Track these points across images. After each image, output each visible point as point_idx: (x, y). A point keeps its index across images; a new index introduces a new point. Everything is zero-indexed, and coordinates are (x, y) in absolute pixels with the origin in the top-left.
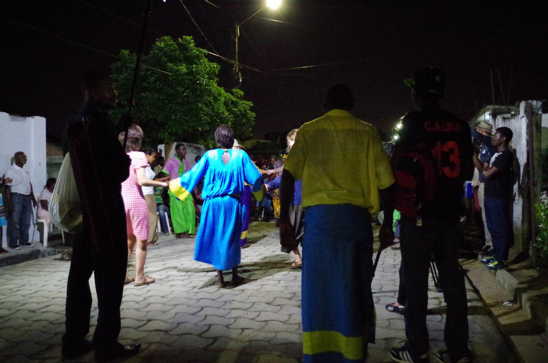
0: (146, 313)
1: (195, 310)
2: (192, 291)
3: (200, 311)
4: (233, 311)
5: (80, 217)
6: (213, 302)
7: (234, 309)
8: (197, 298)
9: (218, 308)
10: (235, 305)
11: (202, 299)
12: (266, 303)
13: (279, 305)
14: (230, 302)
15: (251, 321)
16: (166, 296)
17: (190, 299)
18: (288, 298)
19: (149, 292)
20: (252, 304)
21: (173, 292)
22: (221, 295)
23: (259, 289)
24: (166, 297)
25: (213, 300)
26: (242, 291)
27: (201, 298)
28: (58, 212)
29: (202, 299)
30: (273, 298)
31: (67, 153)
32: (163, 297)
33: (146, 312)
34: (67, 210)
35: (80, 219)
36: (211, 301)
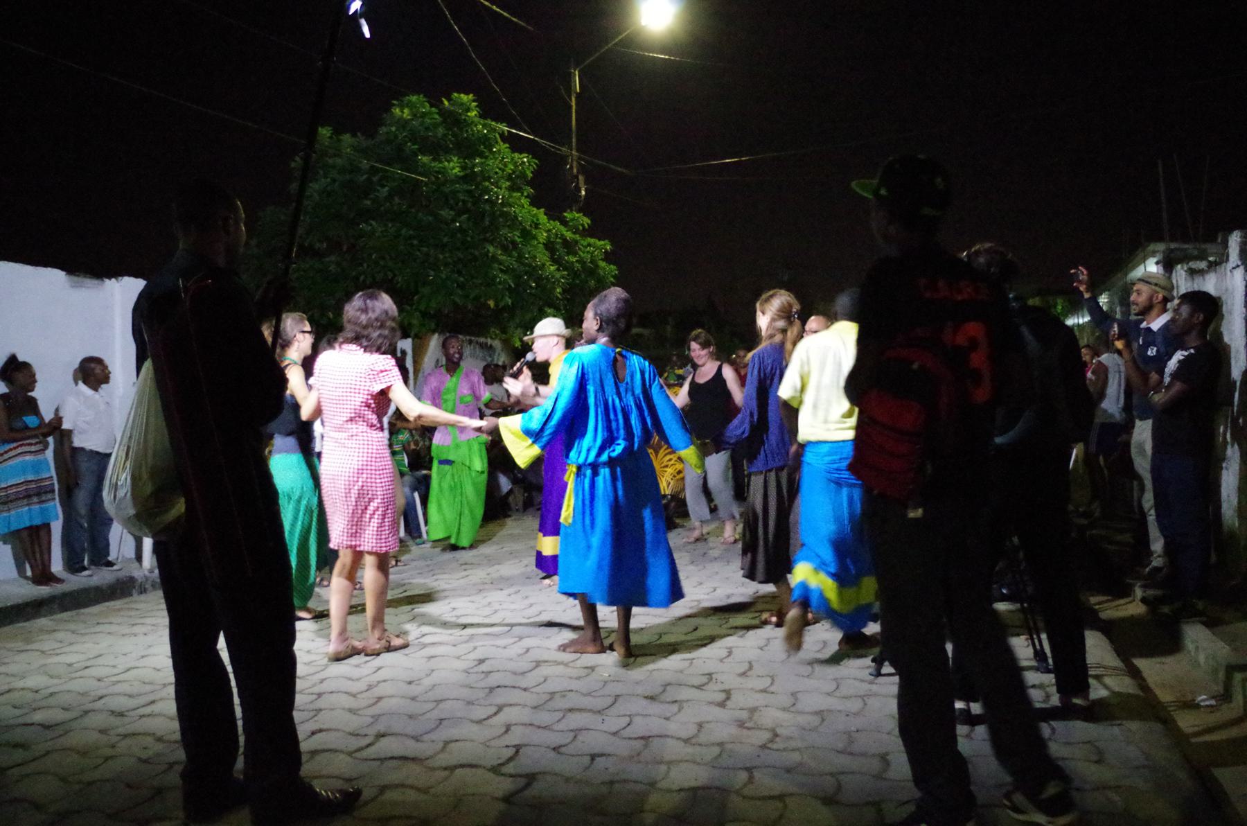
0: (371, 720)
1: (480, 713)
2: (476, 669)
3: (496, 714)
5: (178, 503)
7: (571, 710)
8: (490, 685)
9: (535, 708)
10: (574, 701)
11: (498, 687)
12: (646, 697)
14: (564, 693)
17: (472, 687)
18: (696, 684)
20: (612, 699)
21: (433, 671)
22: (543, 679)
24: (417, 682)
25: (525, 690)
26: (590, 670)
28: (129, 494)
29: (498, 687)
30: (662, 685)
31: (146, 360)
32: (410, 683)
33: (372, 717)
34: (149, 489)
35: (180, 507)
36: (521, 691)
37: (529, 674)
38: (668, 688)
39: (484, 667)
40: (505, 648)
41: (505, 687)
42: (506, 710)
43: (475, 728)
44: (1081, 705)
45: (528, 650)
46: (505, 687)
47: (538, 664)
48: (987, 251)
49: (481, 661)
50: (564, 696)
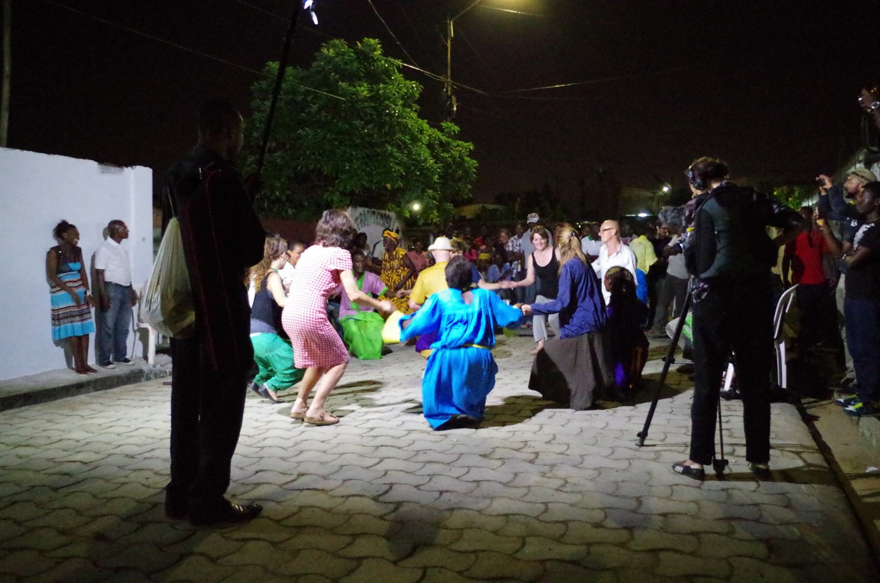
0: (296, 465)
1: (369, 462)
4: (428, 465)
7: (429, 462)
8: (376, 445)
10: (430, 456)
11: (381, 446)
12: (481, 455)
13: (500, 459)
14: (425, 451)
15: (455, 480)
16: (328, 440)
19: (303, 434)
20: (458, 456)
21: (338, 434)
22: (412, 442)
23: (471, 434)
25: (399, 448)
26: (444, 437)
29: (381, 446)
32: (323, 442)
33: (296, 463)
36: (397, 449)
37: (403, 438)
39: (373, 433)
40: (388, 421)
41: (386, 446)
42: (386, 461)
43: (365, 471)
44: (762, 469)
45: (403, 423)
46: (386, 446)
47: (410, 431)
48: (702, 162)
49: (372, 429)
50: (426, 453)
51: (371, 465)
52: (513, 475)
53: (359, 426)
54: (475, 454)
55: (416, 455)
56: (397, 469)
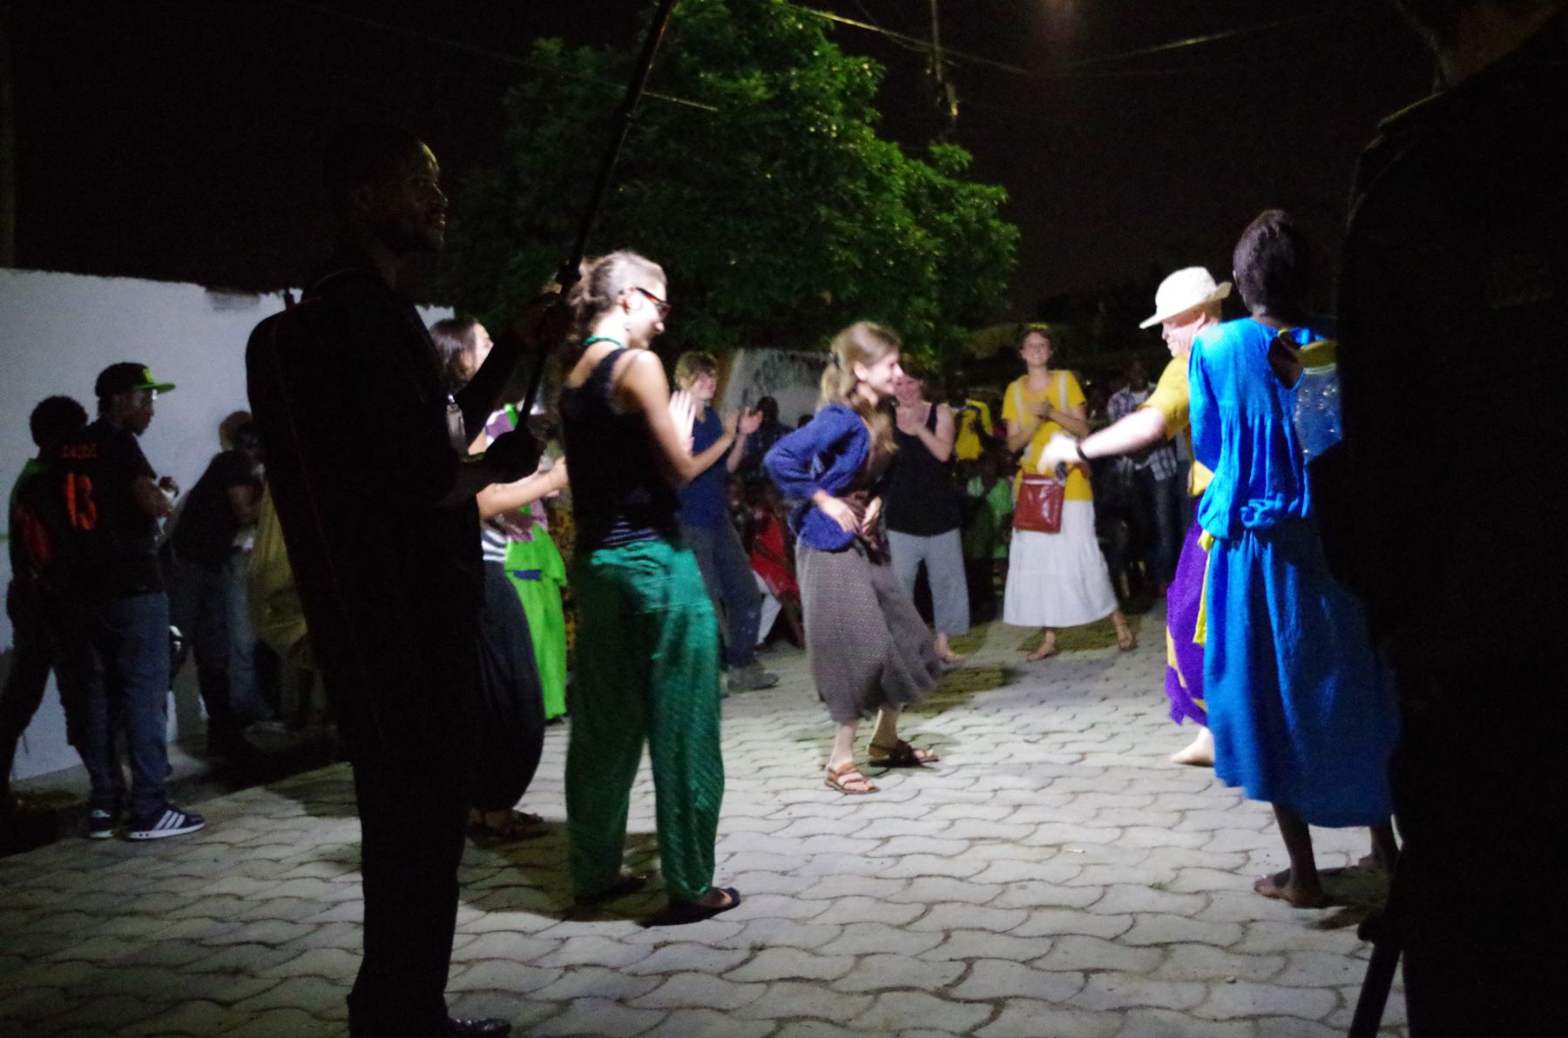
0: (742, 927)
1: (902, 915)
2: (878, 852)
3: (923, 915)
4: (1036, 914)
6: (964, 885)
7: (1037, 907)
8: (905, 874)
9: (982, 905)
10: (1036, 895)
11: (919, 876)
12: (1151, 887)
13: (1197, 893)
14: (1022, 883)
15: (1109, 944)
16: (795, 870)
17: (877, 878)
18: (1226, 867)
19: (733, 859)
20: (1100, 890)
21: (814, 855)
22: (984, 865)
23: (1114, 841)
24: (794, 873)
25: (961, 879)
26: (1055, 850)
27: (918, 873)
29: (919, 876)
30: (1173, 869)
32: (784, 873)
33: (740, 922)
36: (957, 883)
37: (960, 857)
38: (1183, 872)
39: (890, 848)
40: (916, 820)
41: (930, 876)
42: (937, 908)
43: (898, 934)
45: (952, 822)
46: (930, 876)
47: (973, 841)
49: (886, 840)
50: (1023, 888)
51: (909, 920)
52: (1237, 929)
53: (855, 836)
54: (1139, 884)
55: (1003, 892)
56: (970, 925)
